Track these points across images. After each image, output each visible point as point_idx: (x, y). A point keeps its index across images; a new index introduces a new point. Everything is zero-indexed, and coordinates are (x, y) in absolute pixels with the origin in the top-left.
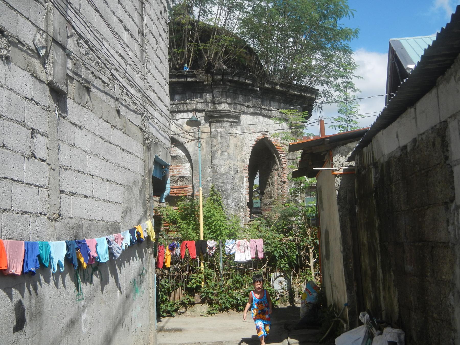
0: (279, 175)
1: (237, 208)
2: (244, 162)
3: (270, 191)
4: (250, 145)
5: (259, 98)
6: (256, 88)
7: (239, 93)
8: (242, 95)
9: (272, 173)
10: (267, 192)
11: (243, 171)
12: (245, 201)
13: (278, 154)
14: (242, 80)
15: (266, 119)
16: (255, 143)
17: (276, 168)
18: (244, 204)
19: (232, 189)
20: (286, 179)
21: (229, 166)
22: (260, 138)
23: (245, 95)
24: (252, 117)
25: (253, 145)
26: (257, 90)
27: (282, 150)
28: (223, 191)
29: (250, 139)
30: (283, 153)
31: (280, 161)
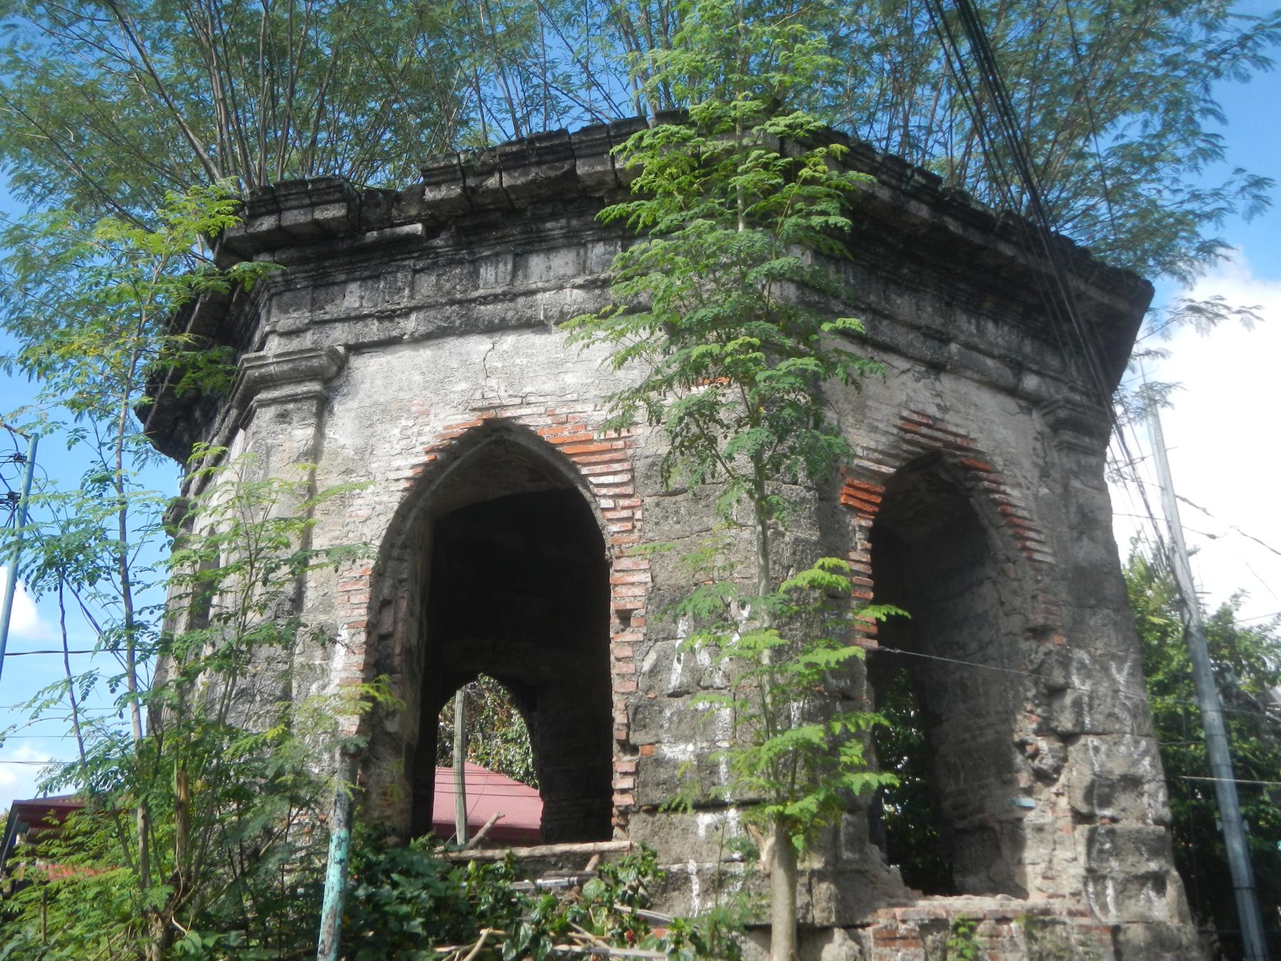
4: (392, 476)
5: (452, 263)
6: (407, 229)
7: (343, 277)
8: (363, 279)
11: (339, 600)
14: (294, 217)
15: (509, 341)
16: (425, 459)
22: (458, 431)
23: (376, 277)
24: (425, 354)
25: (410, 473)
26: (411, 237)
27: (607, 457)
29: (398, 448)
30: (617, 467)
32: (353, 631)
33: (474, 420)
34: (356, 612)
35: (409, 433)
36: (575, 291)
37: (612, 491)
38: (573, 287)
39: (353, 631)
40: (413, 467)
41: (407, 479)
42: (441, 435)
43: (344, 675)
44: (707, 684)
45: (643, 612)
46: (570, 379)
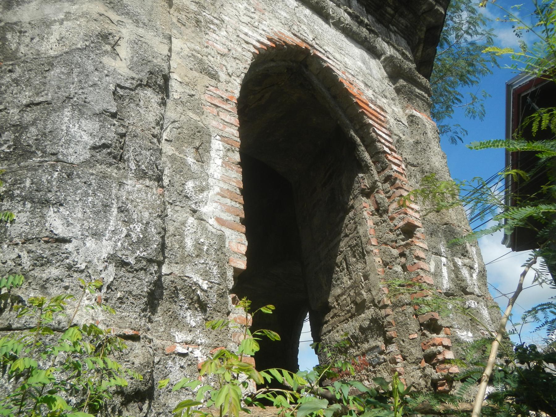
0: (380, 210)
1: (142, 284)
2: (214, 76)
3: (355, 286)
4: (242, 36)
9: (351, 214)
10: (337, 298)
11: (208, 109)
12: (221, 263)
13: (364, 129)
17: (366, 183)
18: (206, 275)
19: (112, 152)
20: (414, 217)
21: (96, 27)
22: (289, 42)
25: (258, 45)
27: (379, 122)
28: (27, 153)
29: (246, 19)
30: (384, 130)
31: (378, 155)
32: (228, 147)
33: (298, 41)
34: (228, 129)
35: (253, 15)
36: (346, 14)
37: (387, 144)
38: (346, 11)
39: (228, 147)
40: (259, 41)
41: (255, 47)
42: (275, 34)
43: (226, 187)
44: (472, 291)
45: (422, 230)
46: (349, 62)
